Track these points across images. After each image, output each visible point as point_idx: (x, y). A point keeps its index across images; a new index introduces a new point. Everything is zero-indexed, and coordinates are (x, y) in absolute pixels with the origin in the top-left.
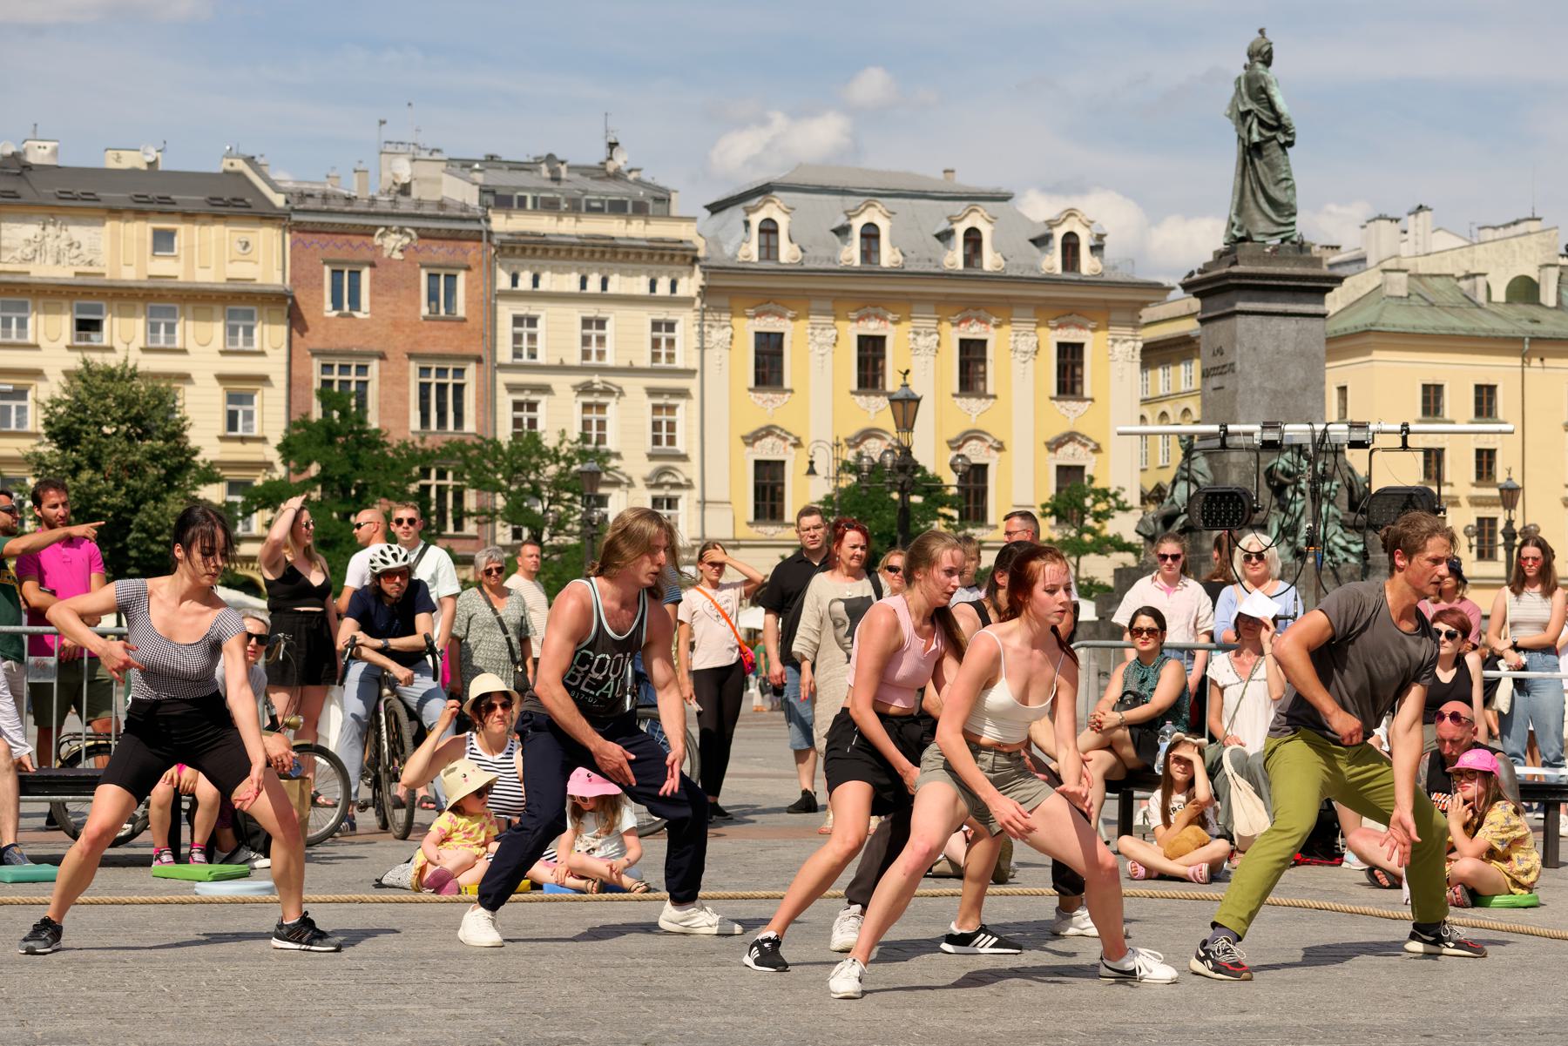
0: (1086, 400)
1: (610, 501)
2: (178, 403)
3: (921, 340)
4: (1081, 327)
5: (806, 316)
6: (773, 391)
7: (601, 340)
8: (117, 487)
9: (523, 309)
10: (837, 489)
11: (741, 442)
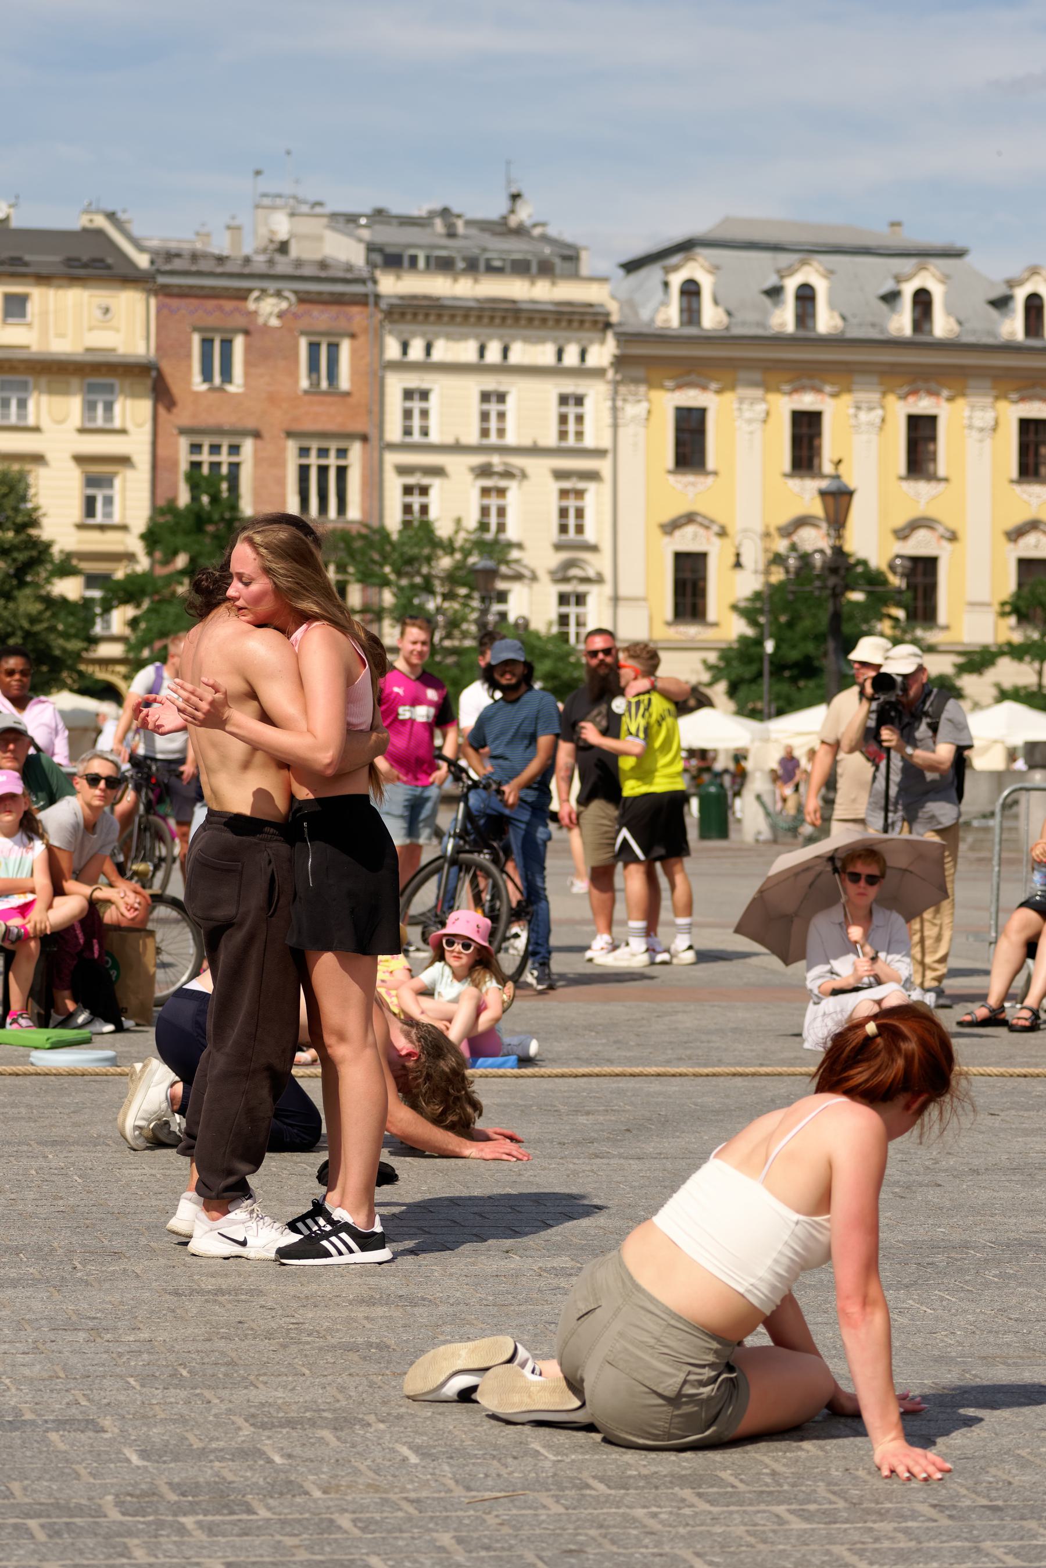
1: (512, 598)
2: (32, 491)
3: (863, 416)
7: (501, 416)
9: (414, 381)
11: (658, 532)
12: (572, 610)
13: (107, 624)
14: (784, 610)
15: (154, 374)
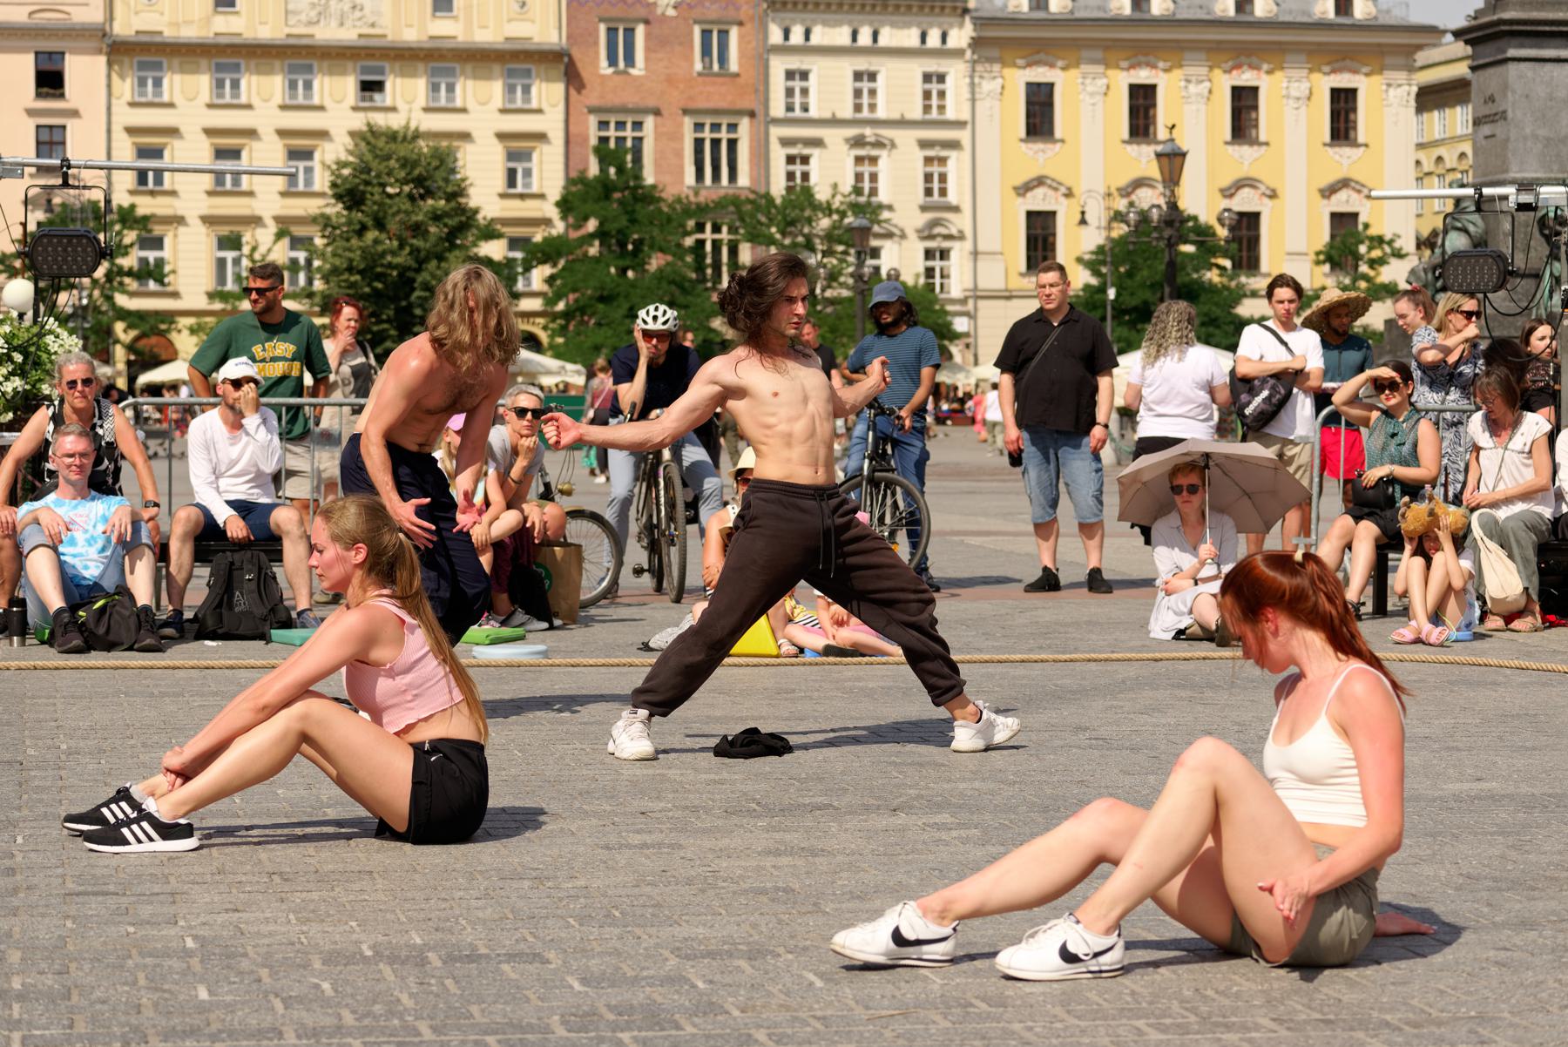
0: (1359, 146)
1: (883, 253)
2: (460, 163)
3: (1192, 88)
4: (1355, 72)
5: (1077, 65)
6: (1045, 142)
7: (873, 92)
8: (401, 246)
9: (795, 63)
10: (1108, 238)
11: (1013, 194)
12: (937, 264)
13: (528, 282)
14: (1123, 263)
15: (566, 59)
